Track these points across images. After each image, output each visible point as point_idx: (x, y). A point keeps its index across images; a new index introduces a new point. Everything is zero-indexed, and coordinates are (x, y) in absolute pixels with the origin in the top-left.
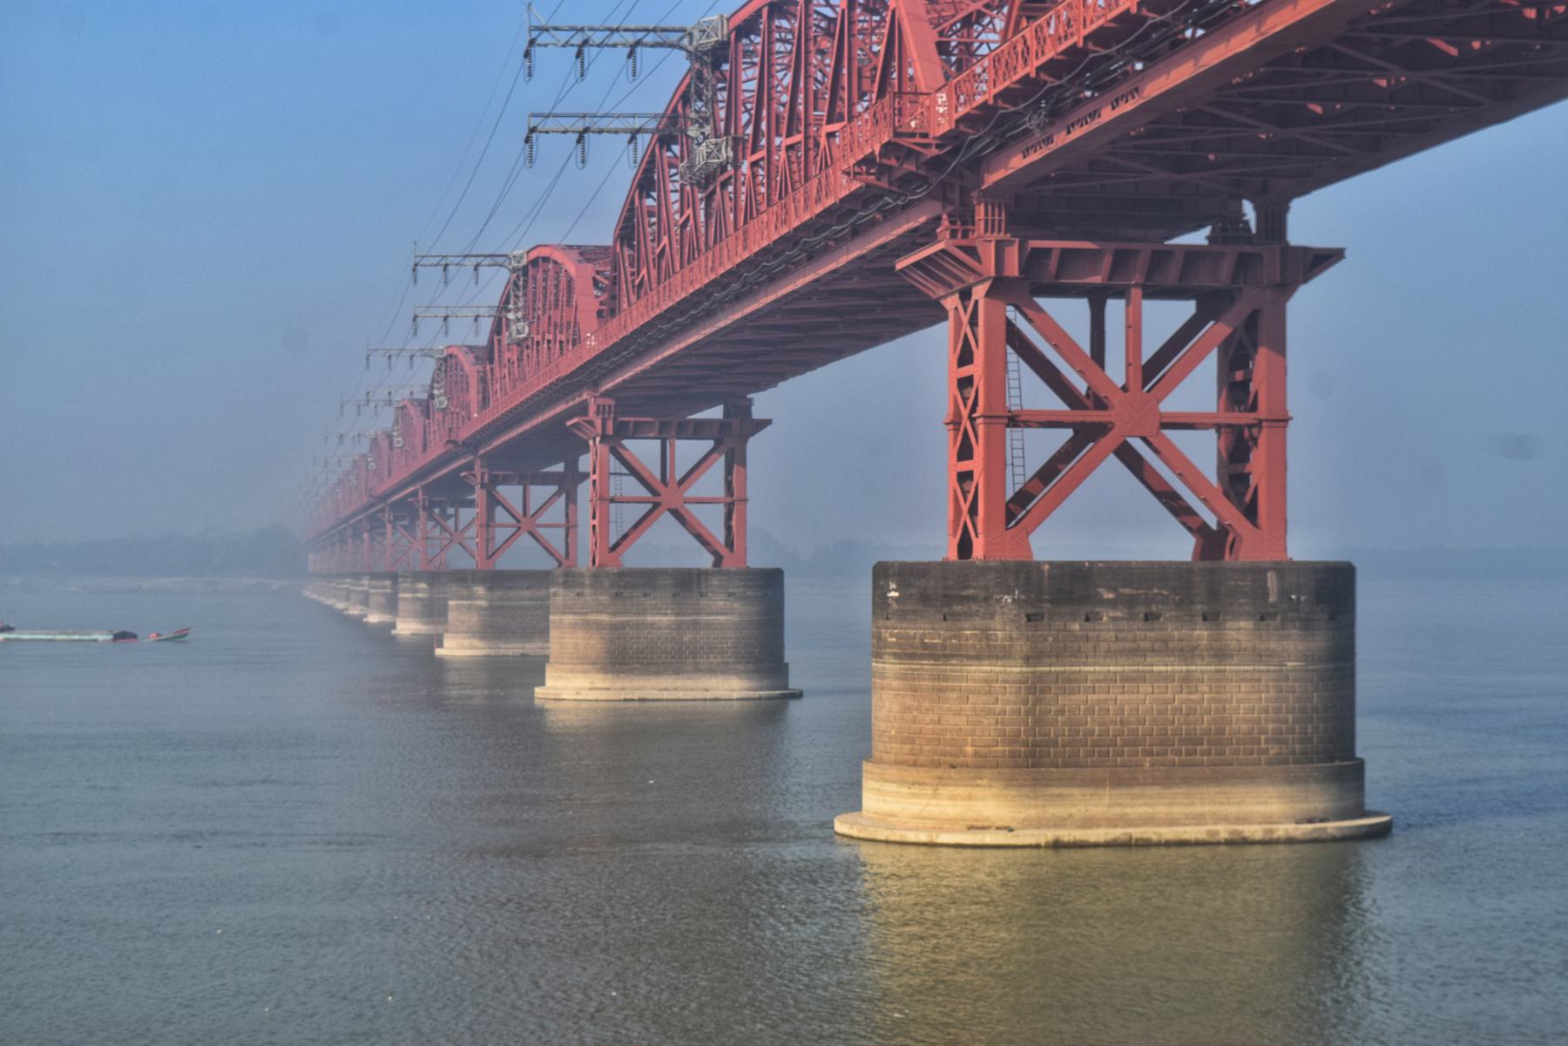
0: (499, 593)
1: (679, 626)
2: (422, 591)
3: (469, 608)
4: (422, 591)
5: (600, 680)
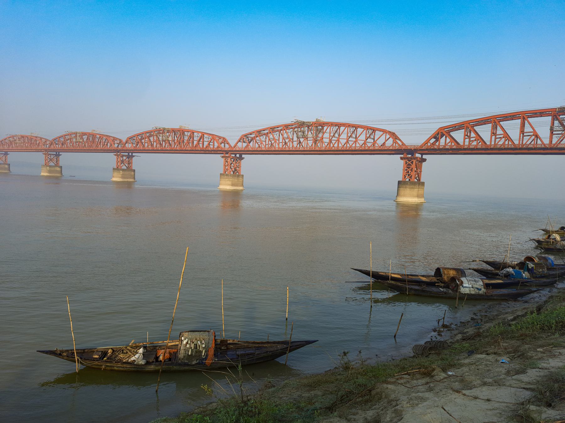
0: (124, 172)
1: (237, 181)
2: (48, 168)
3: (119, 174)
4: (48, 168)
5: (231, 187)
